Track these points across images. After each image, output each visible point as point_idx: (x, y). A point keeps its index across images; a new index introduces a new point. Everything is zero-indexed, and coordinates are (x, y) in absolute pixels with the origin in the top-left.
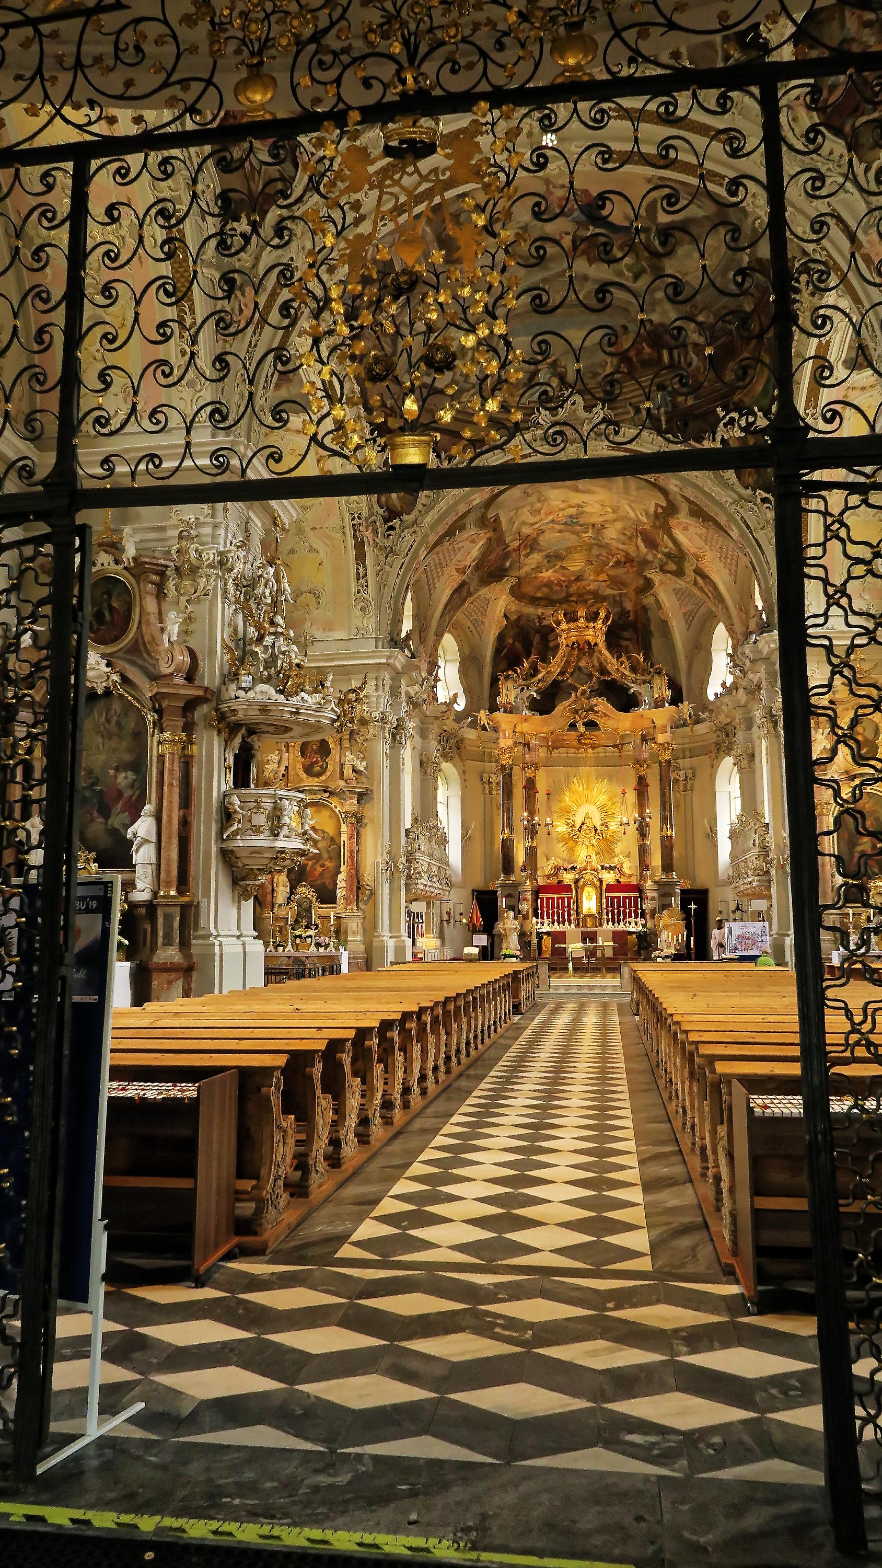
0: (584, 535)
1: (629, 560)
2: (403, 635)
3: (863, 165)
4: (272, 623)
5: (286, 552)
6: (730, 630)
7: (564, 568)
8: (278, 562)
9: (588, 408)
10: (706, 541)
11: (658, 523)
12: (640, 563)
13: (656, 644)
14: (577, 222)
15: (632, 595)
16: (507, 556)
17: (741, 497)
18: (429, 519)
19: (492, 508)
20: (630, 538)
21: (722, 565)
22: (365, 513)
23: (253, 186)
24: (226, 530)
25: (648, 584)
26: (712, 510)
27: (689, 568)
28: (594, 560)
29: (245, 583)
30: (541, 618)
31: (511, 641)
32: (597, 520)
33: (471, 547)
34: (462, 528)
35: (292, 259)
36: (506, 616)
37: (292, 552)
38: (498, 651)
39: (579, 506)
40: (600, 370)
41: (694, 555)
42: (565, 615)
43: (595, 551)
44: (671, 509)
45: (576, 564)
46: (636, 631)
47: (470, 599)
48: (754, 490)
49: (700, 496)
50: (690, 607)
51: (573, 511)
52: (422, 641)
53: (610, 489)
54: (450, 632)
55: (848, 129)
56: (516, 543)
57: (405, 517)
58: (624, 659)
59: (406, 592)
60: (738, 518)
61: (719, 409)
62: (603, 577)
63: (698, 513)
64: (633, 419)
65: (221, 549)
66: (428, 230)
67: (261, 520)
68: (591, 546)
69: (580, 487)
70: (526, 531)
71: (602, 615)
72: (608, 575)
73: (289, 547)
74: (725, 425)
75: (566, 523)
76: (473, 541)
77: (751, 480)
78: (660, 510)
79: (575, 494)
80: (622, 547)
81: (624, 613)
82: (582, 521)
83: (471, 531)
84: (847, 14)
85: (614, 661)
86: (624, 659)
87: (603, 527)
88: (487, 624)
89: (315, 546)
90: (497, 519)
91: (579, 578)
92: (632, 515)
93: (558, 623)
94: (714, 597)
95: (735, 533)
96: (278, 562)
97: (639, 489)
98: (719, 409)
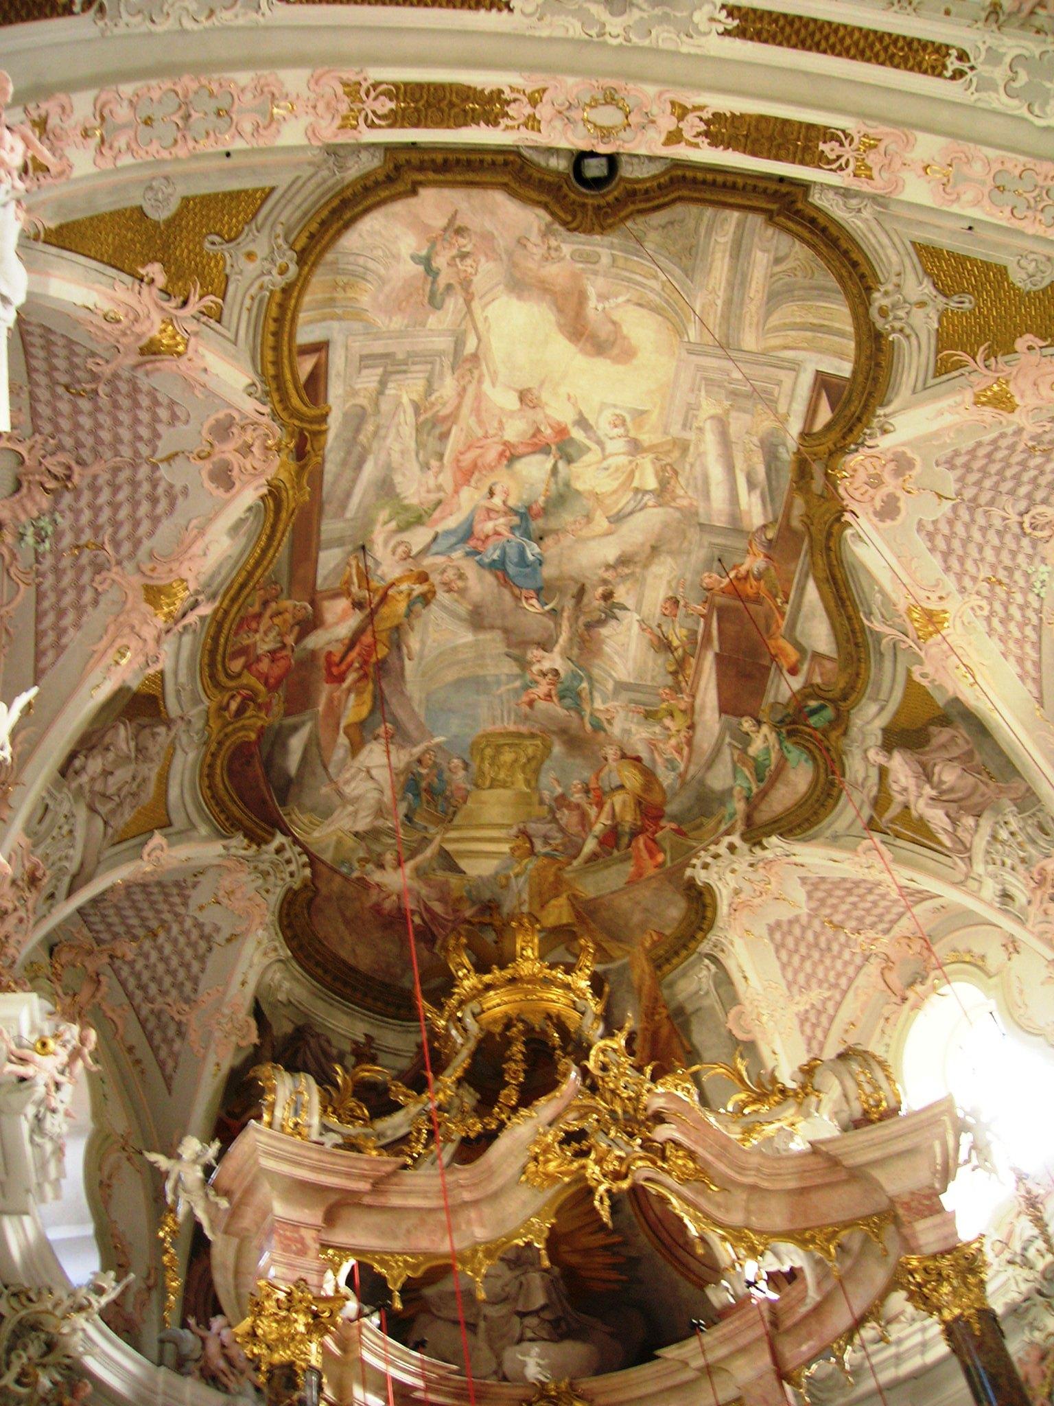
7: (448, 861)
10: (946, 555)
15: (641, 970)
21: (994, 645)
25: (700, 904)
36: (258, 1012)
43: (550, 785)
50: (816, 995)
72: (574, 899)
76: (224, 478)
79: (561, 349)
80: (639, 736)
88: (193, 1036)
94: (962, 805)
97: (774, 298)
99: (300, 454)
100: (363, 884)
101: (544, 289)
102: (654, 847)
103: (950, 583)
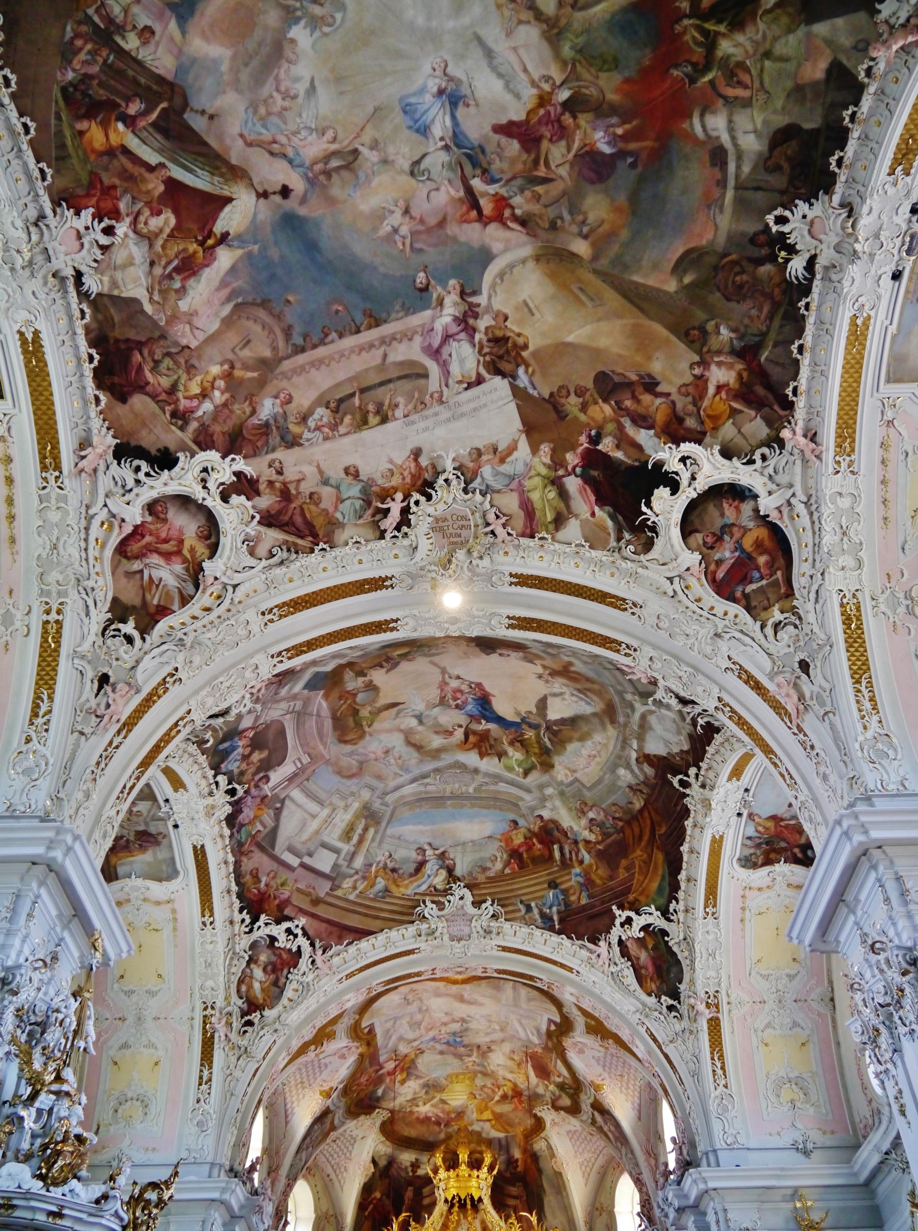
0: (467, 1059)
1: (517, 1093)
2: (248, 1164)
3: (759, 623)
4: (58, 1079)
5: (117, 1046)
6: (638, 1182)
7: (444, 1102)
8: (87, 995)
9: (477, 904)
11: (550, 1044)
12: (529, 1098)
13: (550, 1200)
14: (471, 716)
16: (379, 1080)
17: (644, 1005)
18: (294, 1017)
19: (367, 1015)
20: (519, 1065)
21: (623, 1097)
22: (220, 1003)
23: (148, 597)
24: (24, 941)
25: (539, 1125)
26: (612, 1024)
27: (586, 1102)
28: (477, 1093)
29: (33, 1019)
30: (415, 1165)
31: (378, 1195)
32: (482, 1040)
33: (339, 1062)
34: (331, 1036)
35: (176, 669)
36: (374, 1161)
37: (125, 1046)
38: (362, 1206)
39: (463, 1020)
40: (489, 865)
41: (592, 1084)
42: (444, 1160)
44: (564, 1026)
45: (457, 1097)
46: (526, 1186)
47: (333, 1135)
48: (658, 997)
49: (599, 1006)
50: (587, 1155)
51: (456, 1027)
52: (272, 1171)
53: (498, 1000)
54: (304, 1177)
55: (738, 594)
56: (390, 1066)
57: (267, 1012)
58: (513, 1220)
59: (257, 1107)
60: (643, 1030)
61: (614, 907)
62: (487, 1115)
63: (597, 1028)
64: (523, 918)
65: (10, 963)
66: (324, 704)
67: (79, 948)
68: (475, 1073)
69: (466, 996)
70: (403, 1049)
71: (488, 1160)
72: (493, 1113)
73: (123, 1041)
74: (622, 925)
75: (448, 1043)
77: (653, 987)
78: (553, 1027)
79: (457, 1005)
80: (510, 1076)
81: (511, 1162)
82: (466, 1041)
83: (341, 1041)
84: (725, 505)
85: (502, 1224)
86: (513, 1220)
87: (489, 1049)
89: (154, 1040)
90: (371, 1031)
91: (460, 1114)
92: (522, 1035)
93: (436, 1171)
94: (616, 1139)
95: (640, 1051)
96: (87, 995)
97: (529, 1000)
98: (614, 907)
99: (368, 1044)
100: (411, 1112)
101: (448, 995)
102: (521, 1102)
103: (605, 1075)
